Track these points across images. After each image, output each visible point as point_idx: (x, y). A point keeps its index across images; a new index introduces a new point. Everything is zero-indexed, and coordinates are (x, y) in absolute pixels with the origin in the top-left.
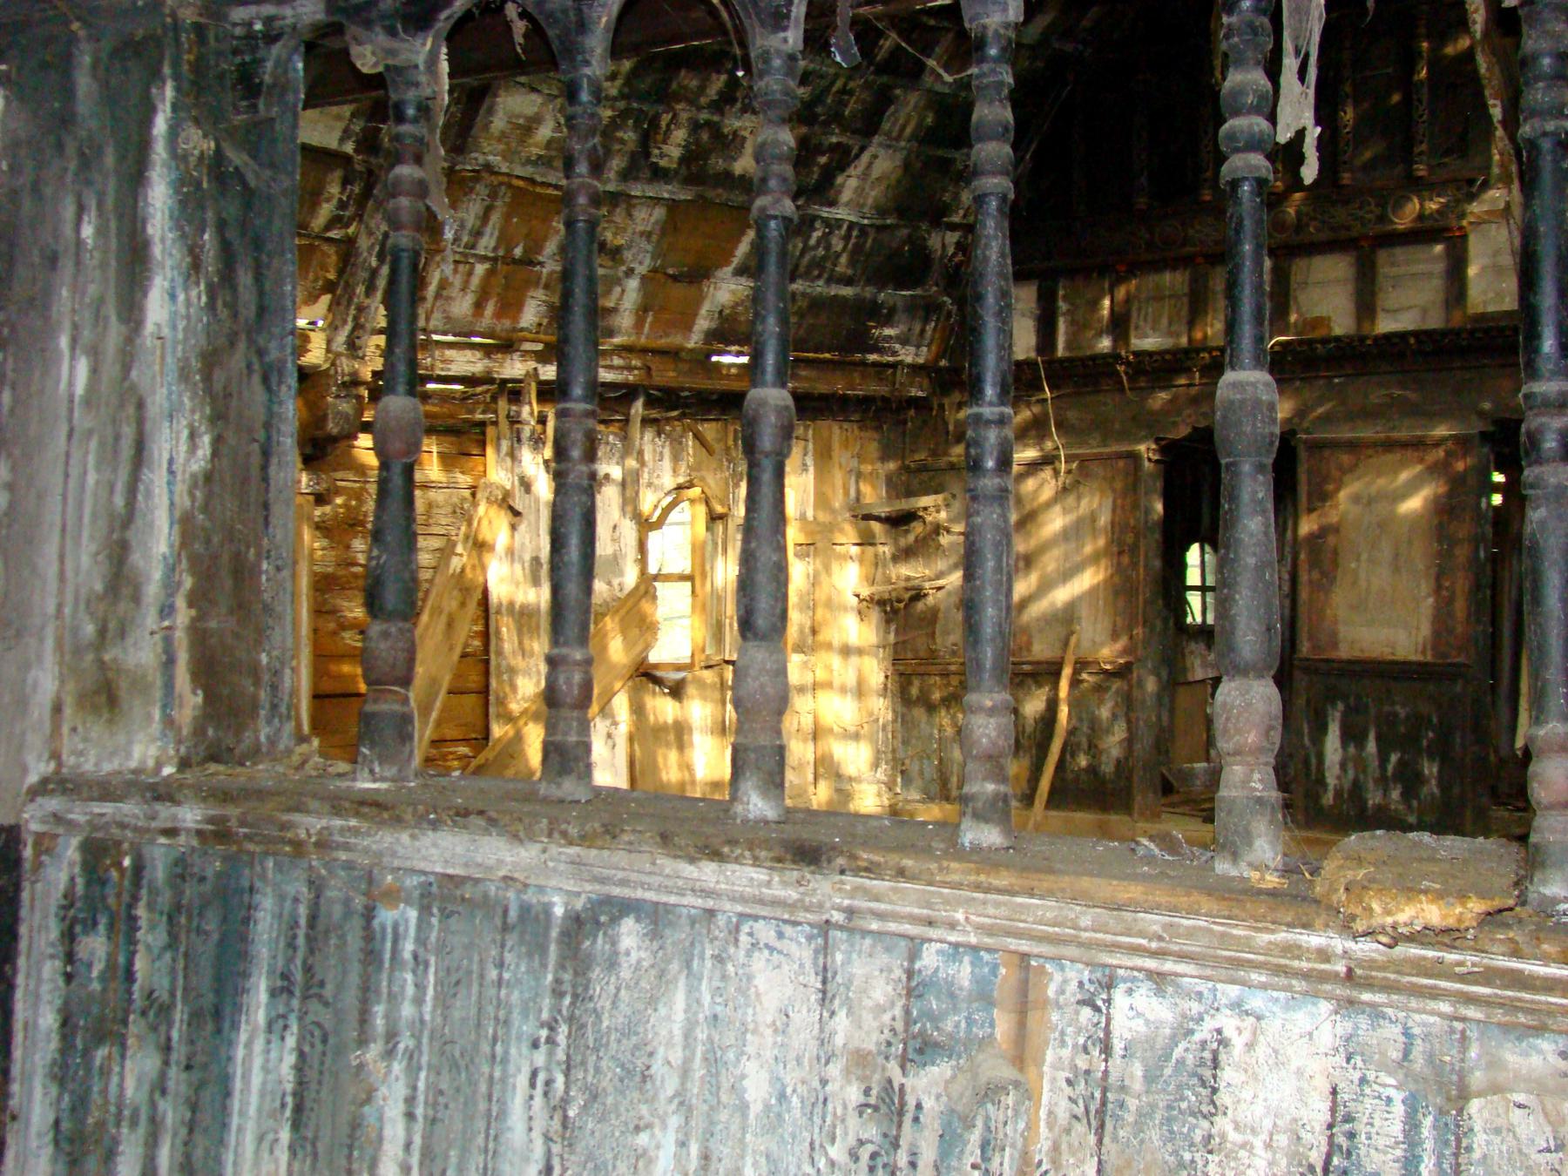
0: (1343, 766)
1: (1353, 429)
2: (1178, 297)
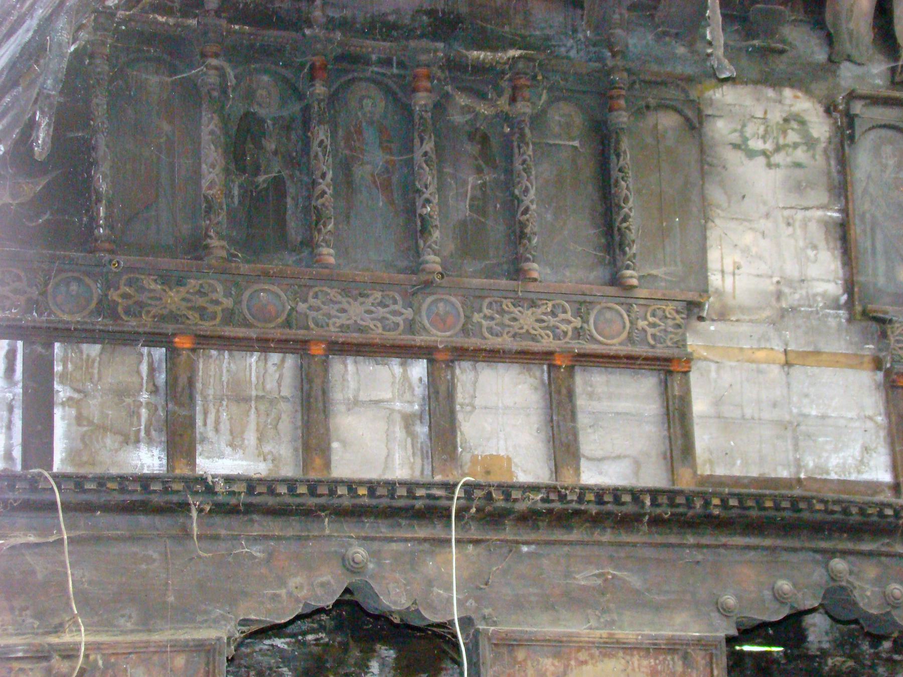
1: (555, 622)
2: (272, 402)
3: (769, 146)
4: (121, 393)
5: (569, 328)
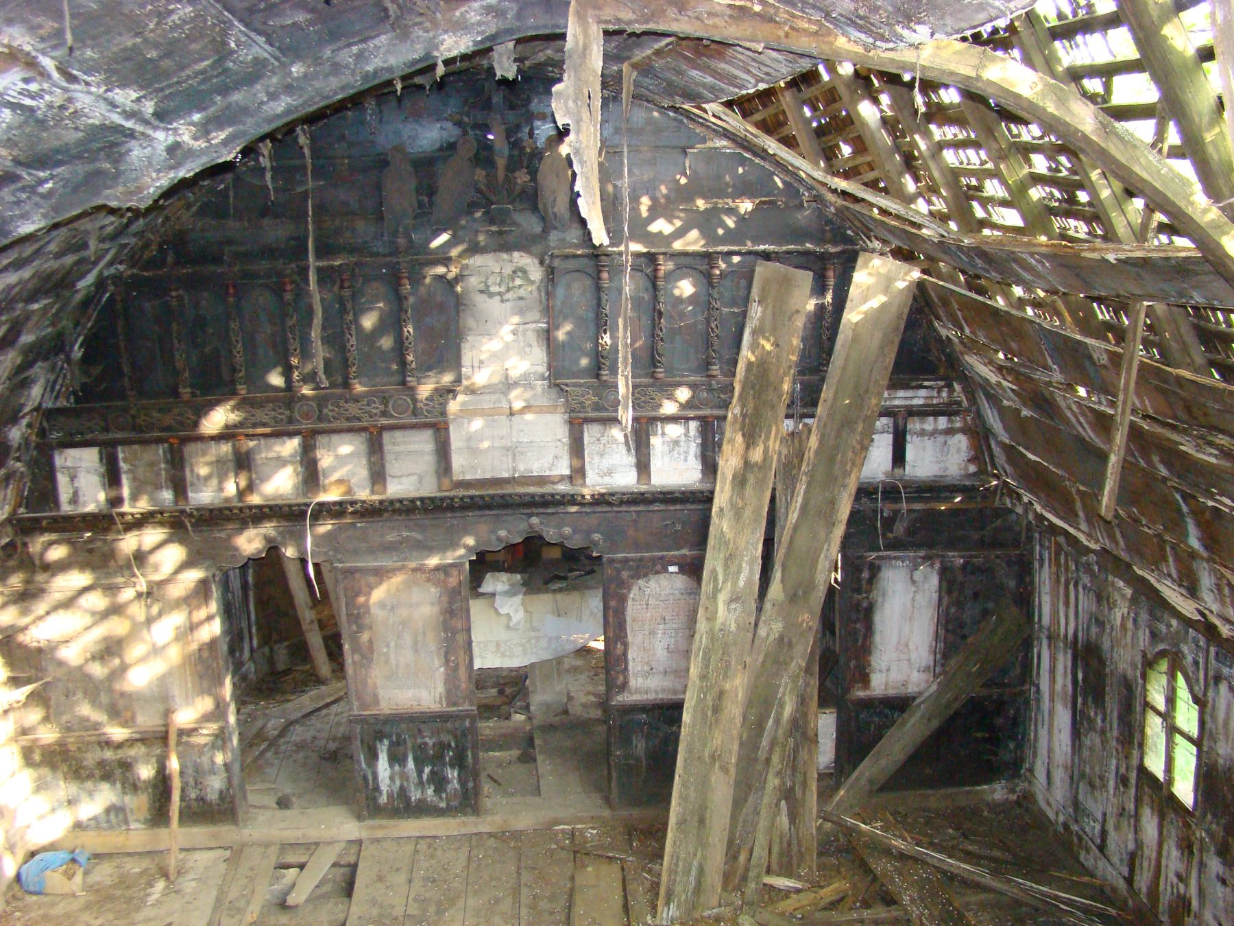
0: (392, 778)
1: (376, 560)
3: (503, 289)
4: (152, 464)
5: (378, 411)
